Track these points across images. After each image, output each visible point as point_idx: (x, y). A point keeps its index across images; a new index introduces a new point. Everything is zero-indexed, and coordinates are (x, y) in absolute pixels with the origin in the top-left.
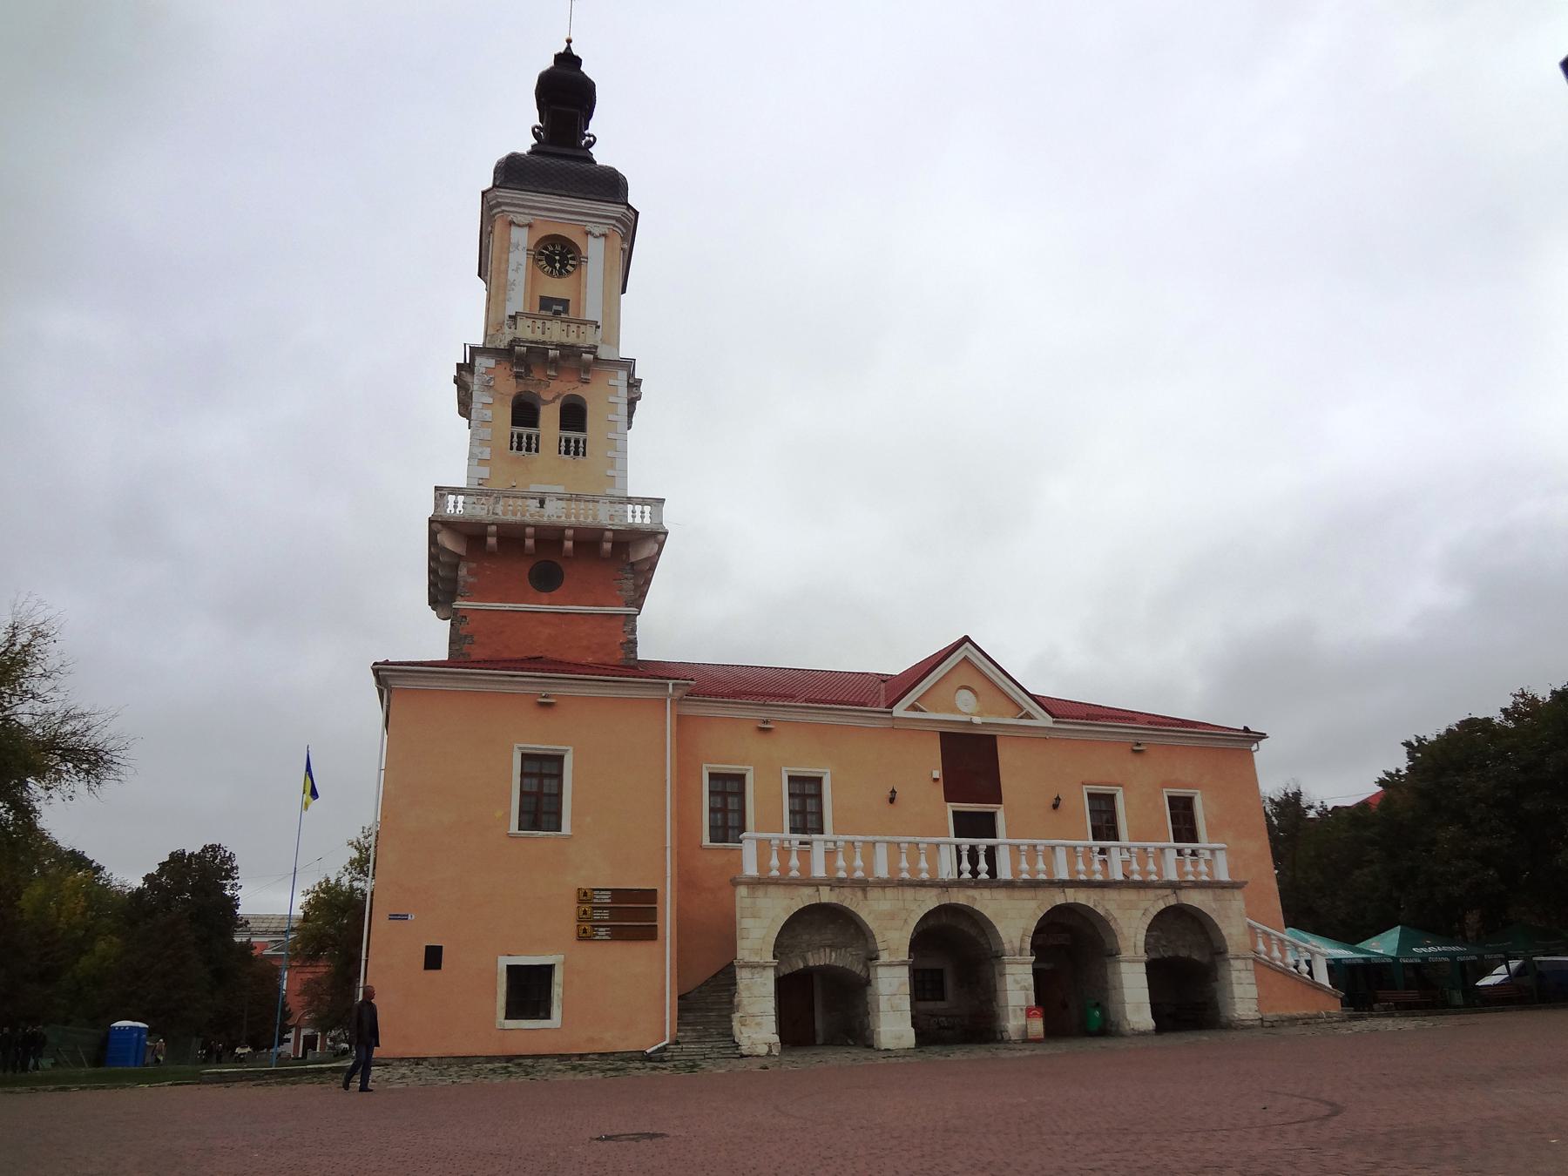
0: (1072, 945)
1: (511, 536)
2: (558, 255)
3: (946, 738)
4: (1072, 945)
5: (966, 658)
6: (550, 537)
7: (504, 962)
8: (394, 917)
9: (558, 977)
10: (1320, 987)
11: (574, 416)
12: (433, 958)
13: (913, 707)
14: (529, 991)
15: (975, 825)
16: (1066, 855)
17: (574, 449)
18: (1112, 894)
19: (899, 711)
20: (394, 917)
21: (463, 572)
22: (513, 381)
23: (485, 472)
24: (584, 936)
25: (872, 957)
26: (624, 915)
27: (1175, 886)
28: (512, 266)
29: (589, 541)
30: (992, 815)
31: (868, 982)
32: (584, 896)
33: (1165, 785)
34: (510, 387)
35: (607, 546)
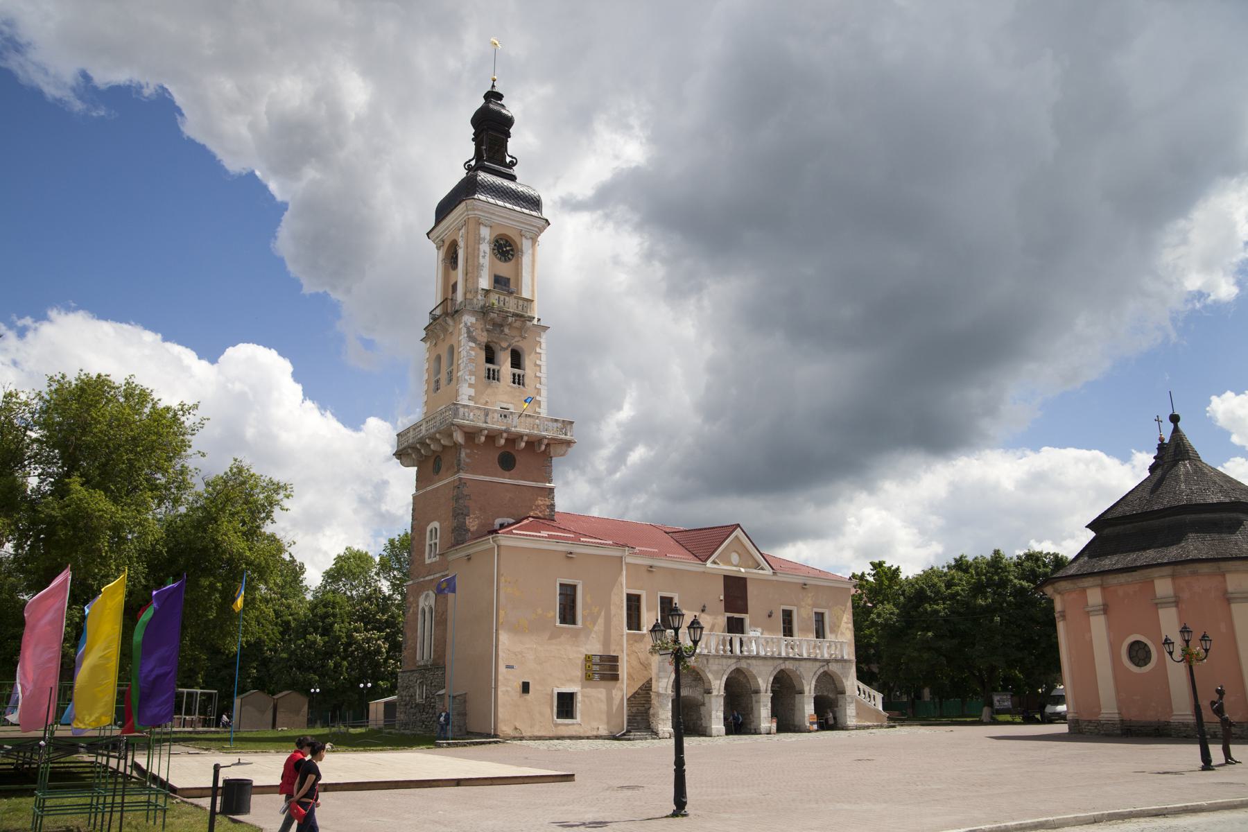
0: (784, 688)
1: (492, 437)
2: (505, 249)
3: (725, 577)
4: (784, 688)
5: (736, 537)
6: (513, 439)
7: (556, 691)
8: (508, 667)
9: (579, 698)
10: (877, 711)
11: (517, 360)
12: (526, 687)
13: (714, 562)
14: (566, 705)
15: (735, 626)
16: (778, 645)
17: (518, 380)
18: (803, 663)
19: (709, 564)
20: (508, 667)
21: (463, 455)
22: (485, 334)
23: (472, 392)
24: (588, 677)
25: (709, 692)
26: (604, 669)
27: (828, 662)
28: (482, 254)
29: (533, 444)
30: (742, 620)
31: (703, 704)
32: (588, 658)
33: (814, 606)
34: (483, 338)
35: (543, 447)
